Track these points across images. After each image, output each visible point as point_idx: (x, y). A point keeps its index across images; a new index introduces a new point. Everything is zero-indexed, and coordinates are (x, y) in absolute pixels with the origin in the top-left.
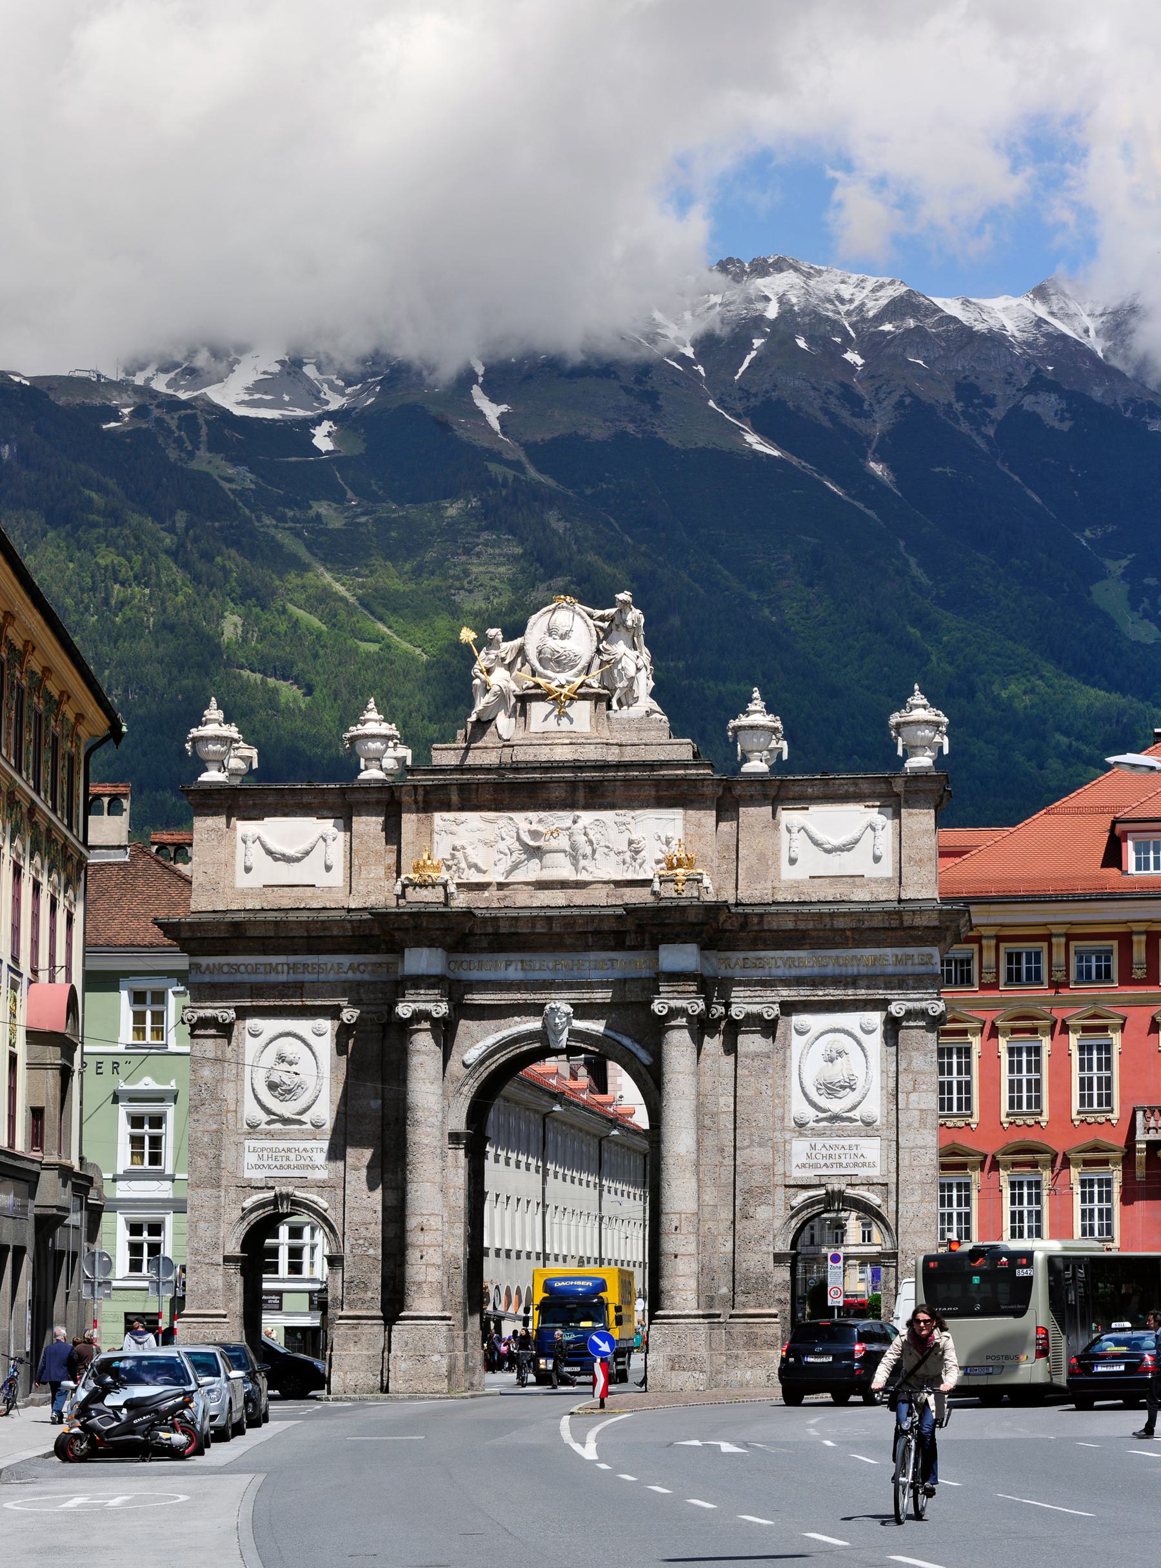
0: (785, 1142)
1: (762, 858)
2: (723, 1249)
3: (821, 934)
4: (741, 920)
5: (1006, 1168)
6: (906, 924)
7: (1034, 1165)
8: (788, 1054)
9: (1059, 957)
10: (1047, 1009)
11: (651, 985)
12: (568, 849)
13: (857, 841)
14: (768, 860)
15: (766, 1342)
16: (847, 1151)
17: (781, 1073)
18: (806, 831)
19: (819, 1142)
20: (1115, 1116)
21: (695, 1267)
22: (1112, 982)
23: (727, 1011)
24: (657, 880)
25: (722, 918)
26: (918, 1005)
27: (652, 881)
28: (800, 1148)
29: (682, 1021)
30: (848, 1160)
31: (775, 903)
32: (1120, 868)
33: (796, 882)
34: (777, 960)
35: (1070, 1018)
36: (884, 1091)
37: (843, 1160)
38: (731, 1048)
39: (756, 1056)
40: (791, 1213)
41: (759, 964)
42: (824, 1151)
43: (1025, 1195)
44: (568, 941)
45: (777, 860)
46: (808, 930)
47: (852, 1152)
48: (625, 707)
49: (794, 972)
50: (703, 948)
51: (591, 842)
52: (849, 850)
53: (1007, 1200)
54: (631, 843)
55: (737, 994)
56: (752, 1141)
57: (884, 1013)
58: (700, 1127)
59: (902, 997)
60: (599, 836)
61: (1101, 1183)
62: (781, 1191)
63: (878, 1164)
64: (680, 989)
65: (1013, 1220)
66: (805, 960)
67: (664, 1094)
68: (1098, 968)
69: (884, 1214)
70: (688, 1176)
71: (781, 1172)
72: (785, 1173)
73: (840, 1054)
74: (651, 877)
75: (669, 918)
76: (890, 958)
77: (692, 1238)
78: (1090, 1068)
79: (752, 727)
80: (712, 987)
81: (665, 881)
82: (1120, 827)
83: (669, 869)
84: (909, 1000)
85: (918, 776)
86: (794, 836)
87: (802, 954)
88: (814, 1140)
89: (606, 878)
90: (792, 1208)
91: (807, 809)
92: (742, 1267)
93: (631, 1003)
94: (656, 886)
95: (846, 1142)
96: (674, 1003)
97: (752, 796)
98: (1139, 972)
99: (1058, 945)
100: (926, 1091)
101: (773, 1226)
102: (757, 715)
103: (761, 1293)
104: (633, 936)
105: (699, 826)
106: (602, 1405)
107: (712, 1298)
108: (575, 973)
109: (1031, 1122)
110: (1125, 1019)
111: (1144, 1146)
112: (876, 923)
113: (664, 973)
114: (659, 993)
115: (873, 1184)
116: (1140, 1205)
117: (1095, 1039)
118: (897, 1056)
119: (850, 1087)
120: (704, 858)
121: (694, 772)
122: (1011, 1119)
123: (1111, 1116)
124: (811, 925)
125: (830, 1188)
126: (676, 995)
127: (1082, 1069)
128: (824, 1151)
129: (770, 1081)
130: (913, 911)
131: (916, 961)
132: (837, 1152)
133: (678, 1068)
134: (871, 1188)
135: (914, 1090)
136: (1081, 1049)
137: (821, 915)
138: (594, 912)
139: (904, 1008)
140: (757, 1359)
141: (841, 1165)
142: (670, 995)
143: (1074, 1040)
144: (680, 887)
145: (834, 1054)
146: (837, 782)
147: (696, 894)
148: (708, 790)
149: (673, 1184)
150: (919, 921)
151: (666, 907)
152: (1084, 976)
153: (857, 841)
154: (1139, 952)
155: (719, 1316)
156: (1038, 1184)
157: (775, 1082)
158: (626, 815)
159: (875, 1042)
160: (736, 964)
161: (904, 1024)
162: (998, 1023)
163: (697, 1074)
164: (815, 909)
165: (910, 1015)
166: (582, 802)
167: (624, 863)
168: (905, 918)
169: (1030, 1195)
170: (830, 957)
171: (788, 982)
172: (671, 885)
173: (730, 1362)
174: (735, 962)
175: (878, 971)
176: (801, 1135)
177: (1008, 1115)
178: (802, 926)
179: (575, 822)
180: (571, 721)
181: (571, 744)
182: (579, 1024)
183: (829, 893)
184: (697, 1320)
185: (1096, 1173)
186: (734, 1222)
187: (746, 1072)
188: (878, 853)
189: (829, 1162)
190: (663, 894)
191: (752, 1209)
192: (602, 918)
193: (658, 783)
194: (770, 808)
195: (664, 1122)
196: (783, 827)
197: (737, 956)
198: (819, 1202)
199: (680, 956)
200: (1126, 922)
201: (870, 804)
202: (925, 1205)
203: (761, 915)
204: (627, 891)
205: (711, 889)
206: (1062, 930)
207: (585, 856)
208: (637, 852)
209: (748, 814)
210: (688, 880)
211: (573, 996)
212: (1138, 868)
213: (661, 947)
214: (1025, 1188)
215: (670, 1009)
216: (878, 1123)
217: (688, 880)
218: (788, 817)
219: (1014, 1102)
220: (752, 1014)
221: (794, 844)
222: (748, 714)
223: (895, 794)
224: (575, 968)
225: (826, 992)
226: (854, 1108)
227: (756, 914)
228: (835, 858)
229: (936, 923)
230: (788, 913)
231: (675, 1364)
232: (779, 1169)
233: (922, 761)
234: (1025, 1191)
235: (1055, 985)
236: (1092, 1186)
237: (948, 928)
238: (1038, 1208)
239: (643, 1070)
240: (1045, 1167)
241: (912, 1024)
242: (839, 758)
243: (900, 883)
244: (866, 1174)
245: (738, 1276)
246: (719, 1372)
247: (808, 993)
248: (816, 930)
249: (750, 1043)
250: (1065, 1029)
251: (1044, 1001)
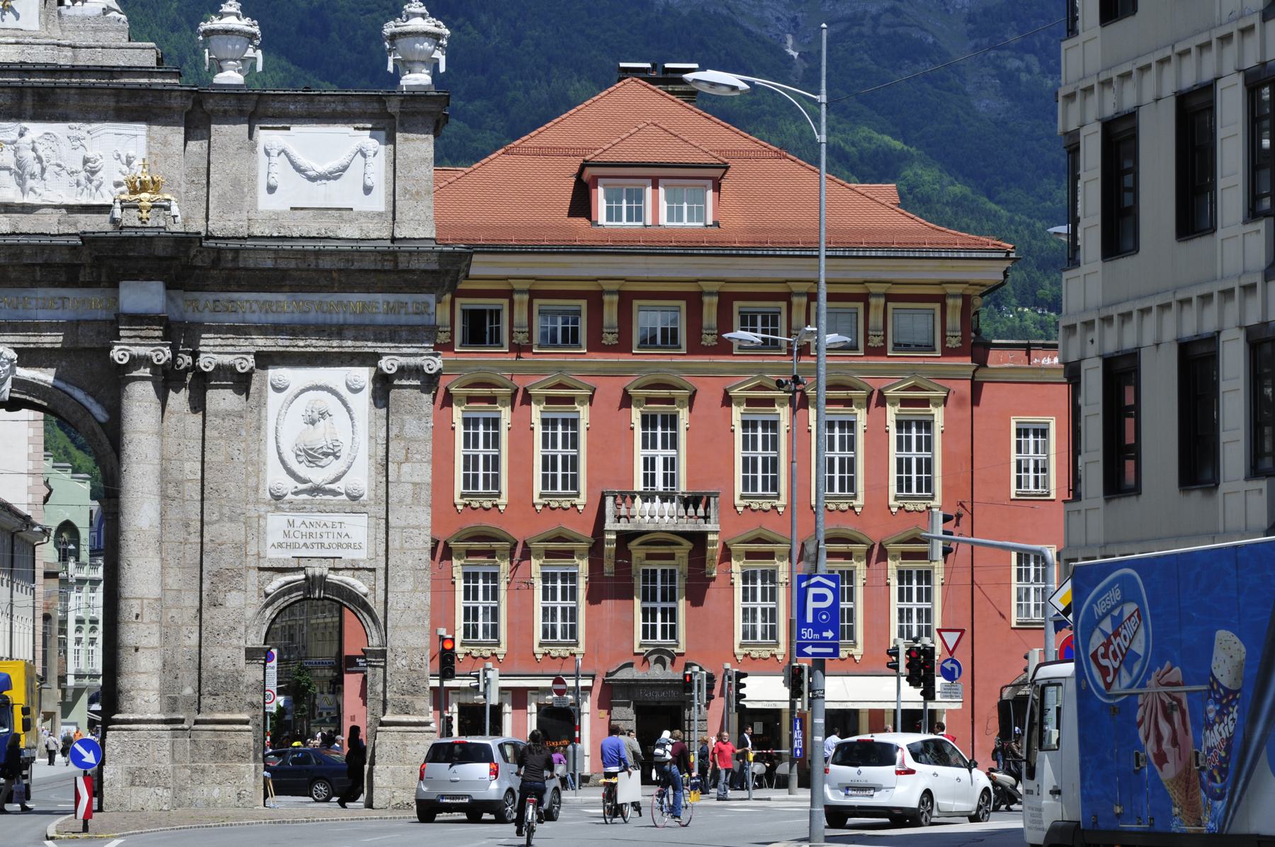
0: (259, 517)
1: (236, 183)
2: (187, 642)
3: (304, 274)
4: (213, 255)
5: (459, 557)
6: (401, 266)
7: (491, 554)
8: (263, 414)
9: (521, 316)
10: (507, 375)
11: (111, 327)
12: (13, 166)
13: (345, 168)
14: (242, 187)
15: (236, 754)
16: (330, 529)
17: (255, 436)
18: (287, 155)
19: (298, 518)
20: (581, 501)
21: (158, 663)
22: (580, 347)
23: (194, 361)
24: (118, 205)
25: (193, 252)
26: (412, 361)
27: (110, 206)
28: (276, 524)
29: (146, 372)
30: (331, 540)
31: (251, 237)
32: (589, 218)
33: (276, 213)
34: (251, 304)
35: (532, 386)
36: (373, 460)
37: (325, 541)
38: (198, 405)
39: (227, 414)
40: (265, 601)
41: (232, 308)
43: (481, 588)
44: (13, 275)
45: (253, 188)
46: (289, 270)
47: (336, 531)
48: (79, 3)
49: (271, 318)
50: (169, 287)
51: (40, 159)
52: (336, 178)
53: (460, 595)
54: (86, 161)
55: (206, 342)
56: (222, 514)
57: (373, 369)
58: (164, 496)
59: (393, 351)
60: (49, 152)
61: (564, 577)
62: (253, 575)
63: (364, 545)
64: (143, 334)
65: (466, 618)
66: (285, 305)
67: (124, 457)
68: (565, 330)
69: (371, 604)
70: (151, 554)
71: (254, 551)
72: (258, 554)
73: (322, 415)
74: (110, 202)
75: (132, 250)
76: (380, 306)
77: (155, 628)
78: (554, 445)
79: (227, 32)
80: (180, 333)
81: (127, 207)
82: (589, 172)
83: (131, 193)
84: (402, 355)
85: (415, 96)
86: (274, 159)
87: (281, 297)
88: (291, 516)
89: (58, 201)
90: (267, 595)
91: (288, 129)
92: (208, 664)
93: (85, 349)
94: (117, 213)
96: (137, 351)
97: (225, 112)
98: (610, 337)
99: (521, 303)
100: (421, 461)
101: (245, 613)
102: (232, 19)
103: (230, 695)
104: (88, 270)
105: (165, 143)
106: (85, 829)
107: (175, 700)
108: (20, 312)
109: (488, 504)
110: (594, 391)
111: (614, 537)
112: (367, 264)
113: (125, 314)
114: (119, 338)
115: (359, 569)
116: (608, 604)
117: (559, 412)
118: (387, 419)
119: (334, 454)
120: (171, 181)
121: (160, 81)
122: (465, 501)
123: (577, 501)
124: (292, 264)
125: (310, 572)
126: (138, 341)
127: (545, 445)
128: (303, 529)
129: (243, 445)
130: (410, 253)
131: (410, 310)
132: (319, 530)
133: (140, 426)
134: (357, 573)
136: (545, 422)
137: (305, 253)
138: (45, 241)
139: (396, 363)
140: (227, 774)
141: (322, 545)
142: (132, 341)
143: (536, 412)
144: (145, 215)
145: (316, 416)
146: (324, 99)
147: (162, 224)
148: (176, 103)
149: (134, 563)
150: (415, 265)
151: (131, 237)
152: (550, 340)
153: (345, 168)
154: (610, 315)
155: (182, 721)
156: (495, 577)
157: (248, 446)
158: (80, 129)
159: (362, 402)
160: (206, 306)
161: (396, 382)
162: (453, 390)
163: (161, 434)
164: (298, 245)
165: (403, 371)
166: (30, 112)
167: (78, 184)
168: (401, 259)
169: (485, 589)
170: (312, 302)
171: (264, 330)
172: (135, 212)
173: (195, 776)
174: (203, 306)
175: (367, 322)
176: (278, 509)
177: (463, 496)
178: (282, 264)
179: (21, 135)
180: (17, 16)
181: (17, 43)
182: (24, 373)
183: (312, 227)
184: (160, 726)
185: (559, 566)
186: (200, 611)
187: (215, 434)
188: (369, 183)
189: (309, 542)
190: (124, 222)
192: (53, 248)
193: (118, 92)
194: (245, 127)
195: (123, 490)
196: (260, 149)
197: (206, 298)
198: (297, 588)
199: (143, 296)
200: (596, 280)
201: (361, 125)
202: (418, 594)
203: (236, 251)
204: (81, 217)
205: (178, 219)
206: (525, 285)
207: (33, 176)
208: (93, 173)
209: (221, 132)
210: (153, 207)
211: (18, 339)
212: (609, 218)
213: (122, 284)
214: (481, 581)
215: (132, 357)
216: (365, 497)
217: (153, 207)
218: (268, 137)
219: (470, 481)
220: (223, 366)
221: (273, 169)
222: (222, 16)
223: (388, 114)
224: (20, 307)
225: (308, 342)
226: (337, 479)
227: (231, 250)
228: (319, 186)
229: (435, 267)
230: (267, 250)
231: (135, 778)
232: (252, 549)
233: (418, 79)
234: (481, 584)
235: (517, 349)
236: (554, 581)
237: (447, 272)
238: (494, 604)
239: (98, 429)
240: (503, 558)
241: (404, 382)
242: (327, 73)
243: (394, 219)
244: (351, 557)
245: (204, 674)
246: (182, 789)
247: (287, 343)
248: (297, 269)
249: (221, 399)
250: (527, 399)
251: (503, 367)
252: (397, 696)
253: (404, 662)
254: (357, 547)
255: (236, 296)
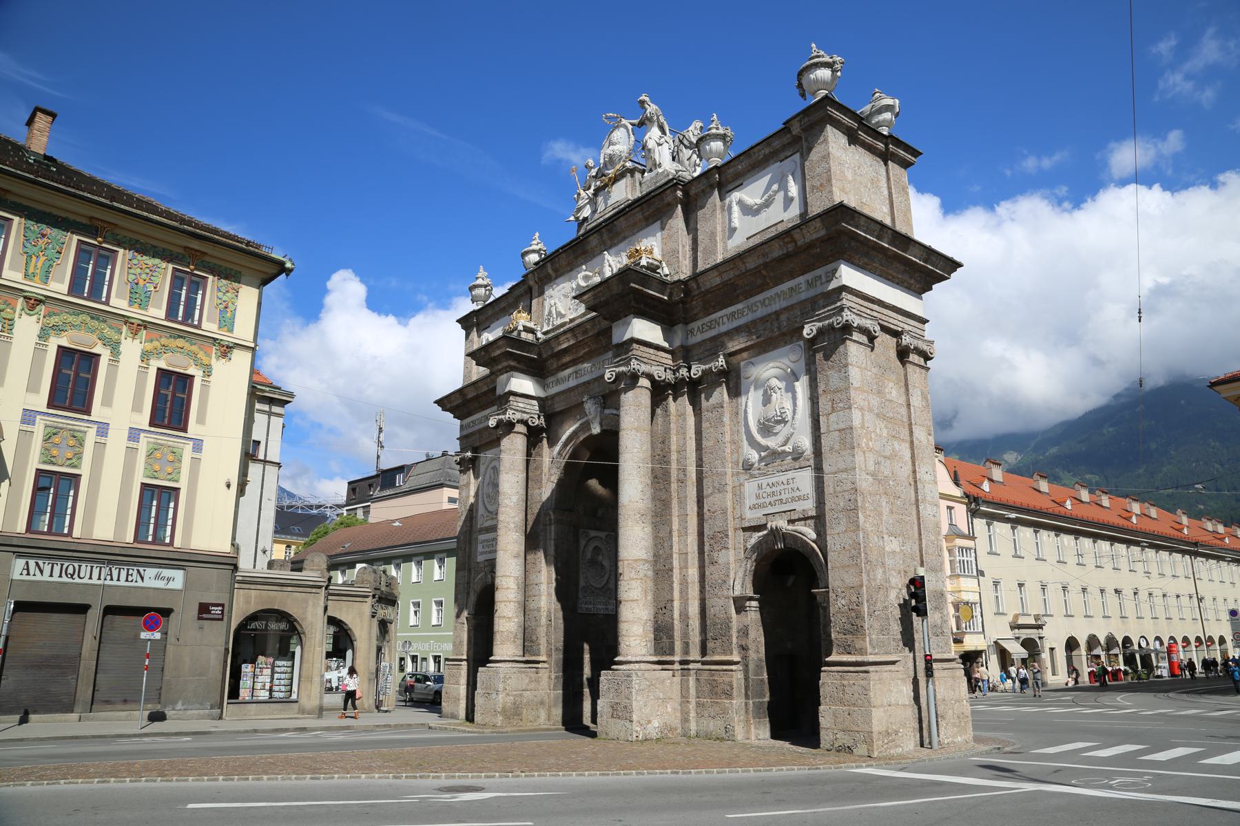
19: (764, 481)
30: (787, 496)
37: (784, 497)
42: (769, 490)
47: (791, 485)
87: (740, 306)
95: (783, 478)
112: (777, 252)
124: (731, 274)
128: (769, 490)
132: (778, 488)
135: (833, 410)
165: (821, 331)
176: (752, 476)
178: (726, 277)
189: (772, 499)
191: (715, 554)
252: (841, 636)
253: (843, 602)
254: (805, 498)
255: (713, 316)
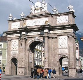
62: (58, 55)
96: (45, 35)
101: (57, 58)
